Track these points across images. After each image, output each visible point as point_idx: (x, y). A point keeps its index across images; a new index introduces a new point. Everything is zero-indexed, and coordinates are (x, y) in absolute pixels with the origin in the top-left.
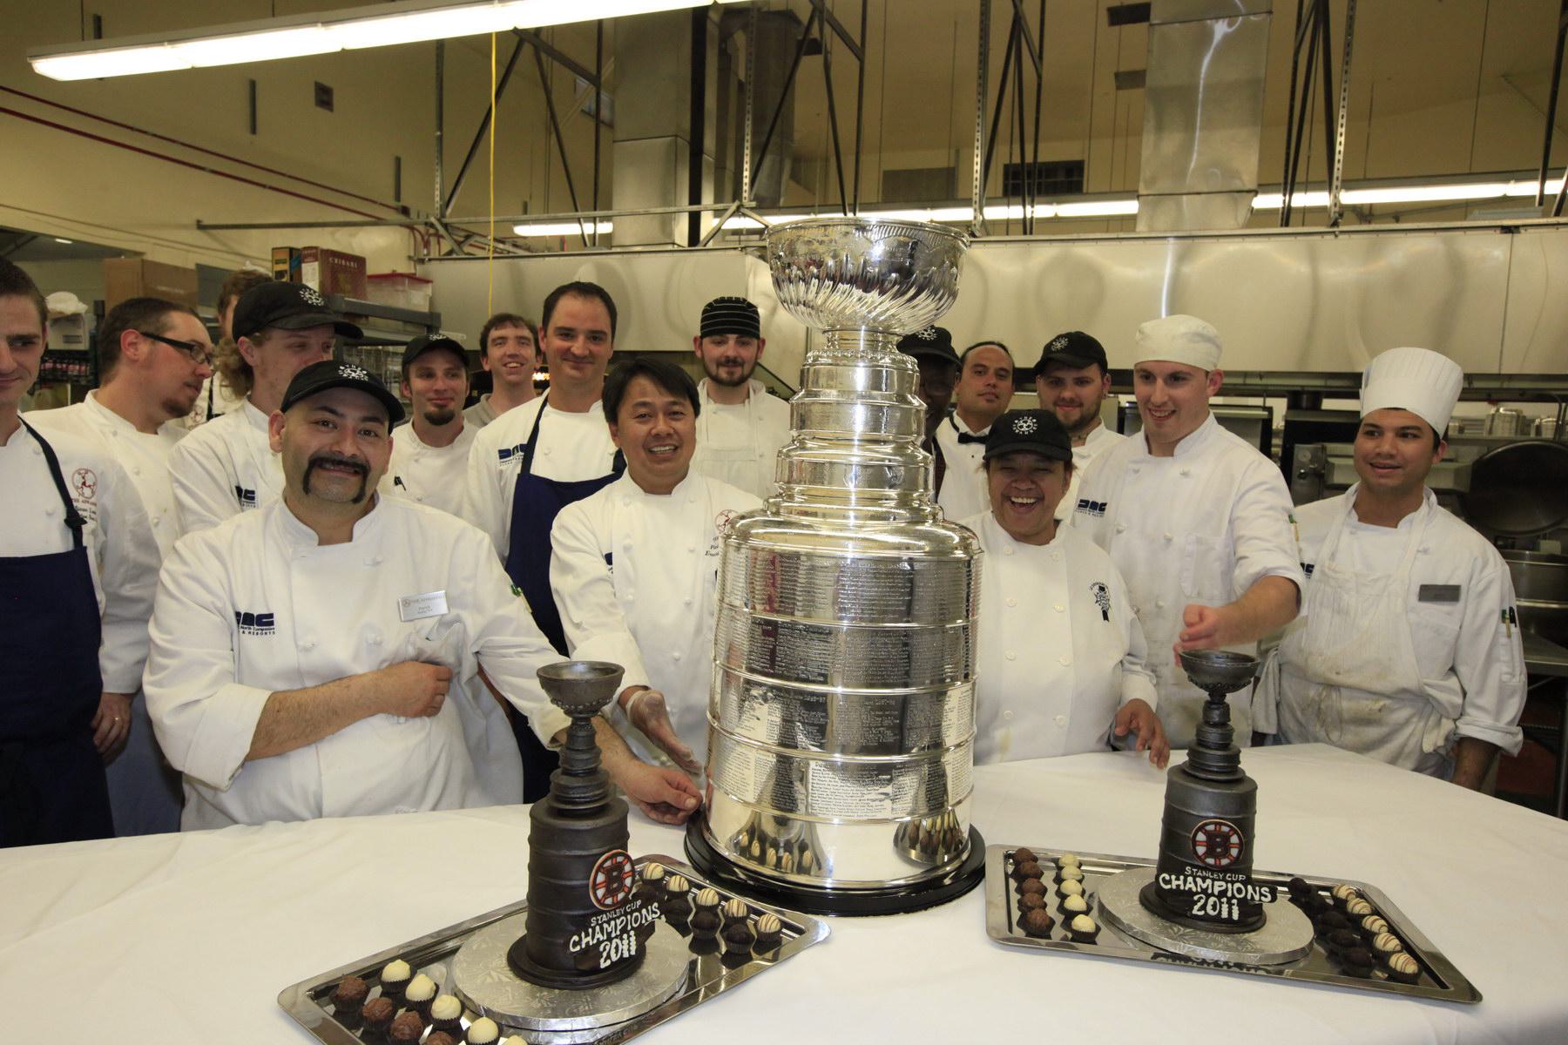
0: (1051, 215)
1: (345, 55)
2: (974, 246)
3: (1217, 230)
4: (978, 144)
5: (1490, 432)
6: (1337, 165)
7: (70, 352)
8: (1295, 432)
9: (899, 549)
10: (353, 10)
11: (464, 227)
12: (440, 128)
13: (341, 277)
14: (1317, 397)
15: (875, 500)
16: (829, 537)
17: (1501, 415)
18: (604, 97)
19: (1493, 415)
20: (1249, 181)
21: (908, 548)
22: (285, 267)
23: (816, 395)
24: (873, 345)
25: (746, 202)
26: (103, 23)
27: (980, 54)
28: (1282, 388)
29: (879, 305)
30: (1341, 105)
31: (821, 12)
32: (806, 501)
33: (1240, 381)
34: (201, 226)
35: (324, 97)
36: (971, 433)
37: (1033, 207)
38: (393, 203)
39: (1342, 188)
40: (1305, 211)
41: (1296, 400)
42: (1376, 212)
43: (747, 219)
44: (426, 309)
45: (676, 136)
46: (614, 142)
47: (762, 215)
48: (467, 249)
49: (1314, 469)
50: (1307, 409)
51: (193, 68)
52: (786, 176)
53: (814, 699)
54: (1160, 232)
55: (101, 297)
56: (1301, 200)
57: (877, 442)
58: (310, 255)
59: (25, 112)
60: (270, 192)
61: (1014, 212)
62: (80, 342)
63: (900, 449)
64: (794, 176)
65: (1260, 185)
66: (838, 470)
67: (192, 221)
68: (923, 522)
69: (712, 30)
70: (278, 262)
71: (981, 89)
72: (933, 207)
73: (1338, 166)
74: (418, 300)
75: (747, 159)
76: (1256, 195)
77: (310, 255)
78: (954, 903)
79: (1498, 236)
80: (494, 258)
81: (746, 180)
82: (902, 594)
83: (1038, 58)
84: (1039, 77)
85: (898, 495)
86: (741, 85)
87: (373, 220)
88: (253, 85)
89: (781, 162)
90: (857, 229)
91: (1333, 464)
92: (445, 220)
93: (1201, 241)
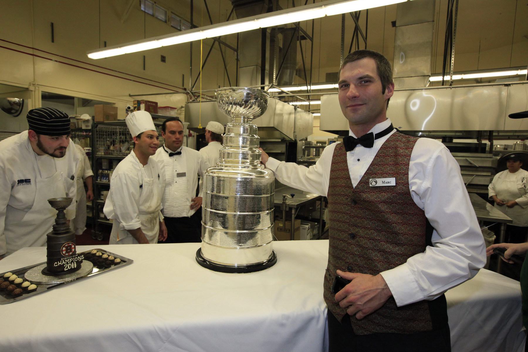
1: (163, 48)
5: (514, 149)
6: (451, 67)
7: (87, 130)
10: (164, 36)
11: (199, 93)
12: (191, 66)
13: (151, 108)
14: (451, 139)
15: (243, 163)
16: (224, 172)
17: (518, 143)
18: (239, 54)
19: (515, 144)
20: (427, 72)
22: (136, 105)
23: (229, 135)
24: (244, 121)
25: (274, 84)
26: (107, 43)
27: (342, 38)
28: (440, 136)
29: (241, 110)
31: (299, 28)
34: (130, 96)
35: (163, 59)
38: (182, 87)
42: (482, 80)
43: (275, 89)
45: (257, 65)
46: (240, 68)
48: (198, 100)
50: (448, 142)
52: (294, 77)
53: (220, 215)
55: (93, 115)
56: (447, 78)
57: (244, 147)
59: (84, 67)
60: (149, 85)
62: (88, 127)
63: (251, 149)
65: (431, 74)
66: (233, 155)
67: (128, 94)
68: (257, 169)
69: (268, 35)
70: (135, 104)
72: (335, 83)
75: (275, 71)
78: (259, 272)
79: (503, 87)
80: (202, 102)
81: (274, 77)
82: (243, 187)
83: (365, 39)
84: (366, 44)
85: (250, 161)
86: (280, 49)
87: (174, 92)
88: (144, 57)
90: (233, 90)
92: (193, 92)
93: (417, 91)
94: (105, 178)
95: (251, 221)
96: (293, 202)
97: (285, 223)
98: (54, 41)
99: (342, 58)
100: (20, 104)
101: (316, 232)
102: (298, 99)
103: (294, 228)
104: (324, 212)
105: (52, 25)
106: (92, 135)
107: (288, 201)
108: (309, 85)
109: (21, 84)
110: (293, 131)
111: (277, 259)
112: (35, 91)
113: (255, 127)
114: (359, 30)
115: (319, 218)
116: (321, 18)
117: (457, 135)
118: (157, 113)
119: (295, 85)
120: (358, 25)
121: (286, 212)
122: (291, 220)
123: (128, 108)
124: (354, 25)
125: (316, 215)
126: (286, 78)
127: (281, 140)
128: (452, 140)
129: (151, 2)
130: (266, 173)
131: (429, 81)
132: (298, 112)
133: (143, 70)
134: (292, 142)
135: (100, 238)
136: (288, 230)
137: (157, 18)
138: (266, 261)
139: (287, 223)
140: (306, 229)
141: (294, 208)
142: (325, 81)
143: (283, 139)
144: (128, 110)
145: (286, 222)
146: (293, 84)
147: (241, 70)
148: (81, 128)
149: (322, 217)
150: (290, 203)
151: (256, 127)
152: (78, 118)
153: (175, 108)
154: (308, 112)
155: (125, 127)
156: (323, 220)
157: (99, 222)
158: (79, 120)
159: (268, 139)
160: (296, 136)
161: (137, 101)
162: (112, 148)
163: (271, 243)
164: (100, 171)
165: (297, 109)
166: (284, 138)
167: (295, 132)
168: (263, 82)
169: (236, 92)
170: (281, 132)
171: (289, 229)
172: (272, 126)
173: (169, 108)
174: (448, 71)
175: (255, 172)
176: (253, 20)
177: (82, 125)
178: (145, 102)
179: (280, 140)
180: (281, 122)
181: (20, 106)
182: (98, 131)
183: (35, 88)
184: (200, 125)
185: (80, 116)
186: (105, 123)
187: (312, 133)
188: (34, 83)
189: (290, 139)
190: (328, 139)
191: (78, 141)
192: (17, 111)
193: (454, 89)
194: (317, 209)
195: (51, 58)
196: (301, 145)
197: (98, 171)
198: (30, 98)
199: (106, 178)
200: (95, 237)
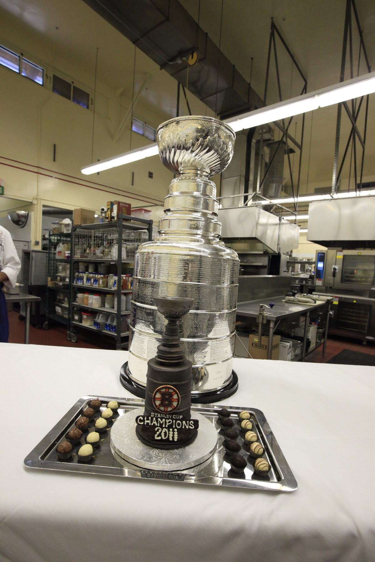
2: (332, 201)
4: (335, 167)
13: (124, 209)
16: (158, 245)
22: (109, 207)
31: (286, 135)
37: (360, 191)
44: (149, 219)
45: (240, 176)
46: (223, 179)
51: (114, 168)
53: (149, 311)
60: (136, 200)
61: (352, 194)
64: (282, 190)
72: (325, 194)
75: (259, 179)
77: (115, 203)
81: (258, 186)
82: (185, 269)
83: (363, 143)
84: (364, 148)
86: (266, 164)
88: (133, 173)
89: (279, 186)
94: (80, 281)
95: (195, 325)
96: (271, 314)
97: (261, 338)
98: (56, 159)
100: (26, 216)
101: (298, 351)
102: (283, 209)
103: (272, 345)
104: (309, 329)
105: (55, 146)
107: (265, 312)
108: (296, 197)
109: (25, 198)
110: (277, 244)
111: (239, 386)
112: (37, 205)
114: (357, 133)
115: (303, 336)
116: (313, 111)
118: (130, 215)
119: (281, 197)
120: (356, 126)
121: (263, 324)
122: (268, 335)
123: (101, 209)
124: (351, 126)
125: (300, 332)
126: (272, 192)
127: (264, 253)
129: (141, 122)
130: (226, 251)
132: (283, 224)
133: (131, 186)
135: (74, 340)
136: (265, 346)
137: (147, 137)
138: (220, 388)
140: (287, 347)
141: (273, 321)
142: (313, 192)
143: (266, 252)
145: (263, 337)
147: (223, 181)
148: (63, 232)
149: (307, 335)
150: (268, 314)
152: (61, 223)
153: (149, 211)
154: (294, 224)
155: (99, 230)
156: (308, 339)
157: (74, 324)
159: (250, 251)
160: (280, 248)
162: (88, 251)
163: (229, 361)
164: (77, 274)
165: (281, 220)
166: (267, 250)
167: (279, 244)
168: (246, 191)
169: (181, 124)
171: (266, 346)
172: (254, 236)
175: (205, 248)
176: (236, 120)
177: (63, 230)
179: (262, 253)
180: (264, 233)
181: (25, 218)
182: (76, 234)
183: (38, 202)
185: (62, 221)
186: (82, 226)
187: (297, 247)
188: (37, 198)
189: (273, 252)
190: (317, 251)
191: (62, 245)
192: (23, 222)
194: (301, 326)
195: (52, 176)
196: (284, 258)
197: (74, 273)
198: (33, 211)
199: (81, 281)
200: (70, 338)
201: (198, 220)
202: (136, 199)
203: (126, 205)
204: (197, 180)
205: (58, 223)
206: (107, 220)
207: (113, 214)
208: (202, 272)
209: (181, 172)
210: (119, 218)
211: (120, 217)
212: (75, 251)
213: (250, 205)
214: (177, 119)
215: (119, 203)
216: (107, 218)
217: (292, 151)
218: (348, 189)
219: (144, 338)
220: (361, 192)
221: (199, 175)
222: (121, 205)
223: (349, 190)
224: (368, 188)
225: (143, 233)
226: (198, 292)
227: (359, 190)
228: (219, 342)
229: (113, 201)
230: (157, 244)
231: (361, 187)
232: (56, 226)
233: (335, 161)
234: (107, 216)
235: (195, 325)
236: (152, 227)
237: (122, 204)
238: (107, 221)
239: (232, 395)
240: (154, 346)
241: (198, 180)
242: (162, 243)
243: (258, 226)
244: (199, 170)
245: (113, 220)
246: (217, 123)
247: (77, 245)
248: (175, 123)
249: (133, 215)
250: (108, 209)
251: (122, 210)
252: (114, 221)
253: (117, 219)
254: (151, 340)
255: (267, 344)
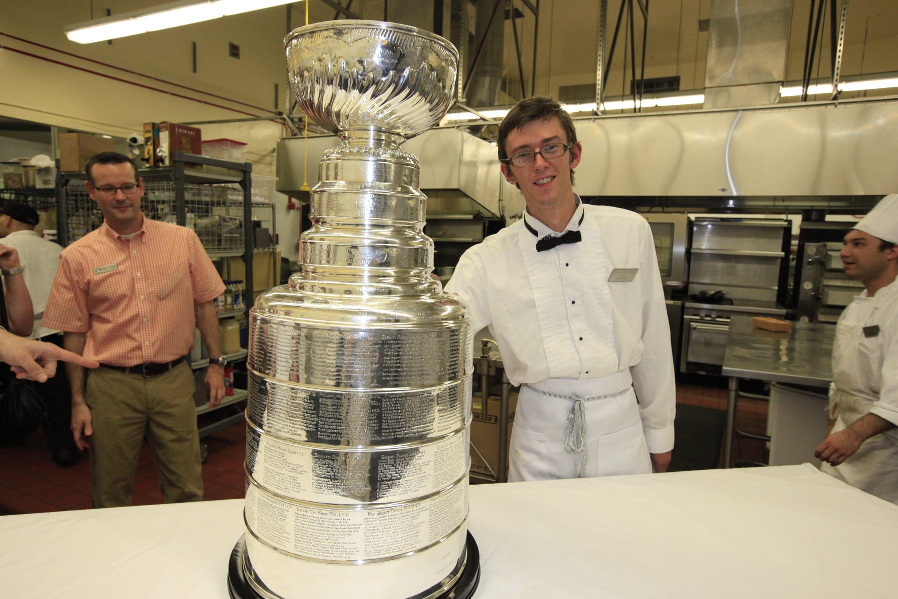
0: (654, 105)
2: (597, 121)
3: (755, 105)
6: (837, 60)
8: (806, 235)
9: (381, 321)
13: (184, 140)
14: (822, 213)
16: (306, 308)
20: (778, 75)
21: (397, 321)
22: (150, 135)
23: (332, 185)
24: (378, 141)
25: (460, 99)
30: (842, 20)
32: (315, 278)
33: (771, 203)
36: (553, 234)
37: (641, 100)
38: (274, 110)
39: (841, 81)
40: (816, 97)
41: (807, 215)
44: (242, 161)
47: (477, 111)
49: (818, 259)
50: (816, 221)
54: (719, 108)
56: (813, 90)
58: (162, 127)
61: (628, 104)
62: (50, 184)
63: (399, 232)
64: (503, 88)
70: (147, 132)
71: (602, 24)
72: (581, 103)
73: (839, 60)
74: (237, 156)
76: (783, 86)
77: (162, 127)
80: (308, 138)
83: (645, 10)
84: (646, 20)
85: (395, 272)
88: (194, 45)
89: (496, 81)
91: (831, 256)
92: (291, 116)
99: (601, 43)
106: (57, 202)
110: (498, 199)
113: (412, 163)
117: (831, 207)
118: (200, 153)
121: (489, 377)
123: (130, 140)
126: (483, 94)
127: (474, 217)
128: (824, 217)
131: (780, 94)
134: (494, 221)
136: (494, 418)
139: (491, 401)
144: (133, 146)
145: (490, 401)
146: (496, 104)
148: (34, 186)
151: (414, 161)
152: (26, 163)
158: (30, 168)
159: (448, 214)
160: (503, 207)
161: (151, 125)
166: (479, 211)
167: (502, 200)
169: (345, 37)
170: (471, 198)
172: (455, 186)
173: (229, 143)
174: (825, 71)
175: (410, 310)
177: (34, 180)
178: (169, 127)
179: (471, 217)
180: (473, 179)
182: (69, 192)
184: (305, 184)
185: (30, 160)
189: (490, 215)
193: (843, 106)
201: (387, 247)
202: (205, 103)
203: (188, 132)
204: (384, 155)
205: (18, 163)
206: (147, 165)
207: (161, 151)
208: (407, 363)
209: (347, 134)
210: (175, 162)
211: (177, 159)
212: (70, 230)
213: (445, 124)
214: (337, 25)
215: (172, 128)
216: (147, 160)
217: (518, 14)
218: (621, 94)
219: (286, 508)
220: (643, 101)
221: (383, 142)
222: (178, 131)
223: (623, 97)
224: (652, 95)
225: (229, 192)
226: (401, 406)
227: (639, 96)
228: (445, 497)
229: (158, 120)
230: (306, 304)
231: (643, 90)
232: (11, 170)
233: (600, 46)
234: (146, 156)
235: (396, 473)
236: (250, 179)
237: (180, 130)
238: (147, 168)
239: (472, 595)
240: (310, 527)
241: (387, 156)
242: (314, 302)
243: (461, 168)
244: (384, 132)
245: (161, 165)
246: (425, 39)
247: (73, 215)
248: (332, 31)
249: (206, 151)
250: (147, 140)
251: (181, 143)
252: (162, 167)
253: (170, 163)
254: (302, 513)
255: (498, 415)
